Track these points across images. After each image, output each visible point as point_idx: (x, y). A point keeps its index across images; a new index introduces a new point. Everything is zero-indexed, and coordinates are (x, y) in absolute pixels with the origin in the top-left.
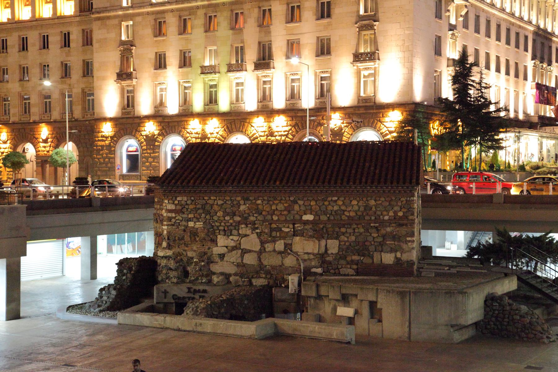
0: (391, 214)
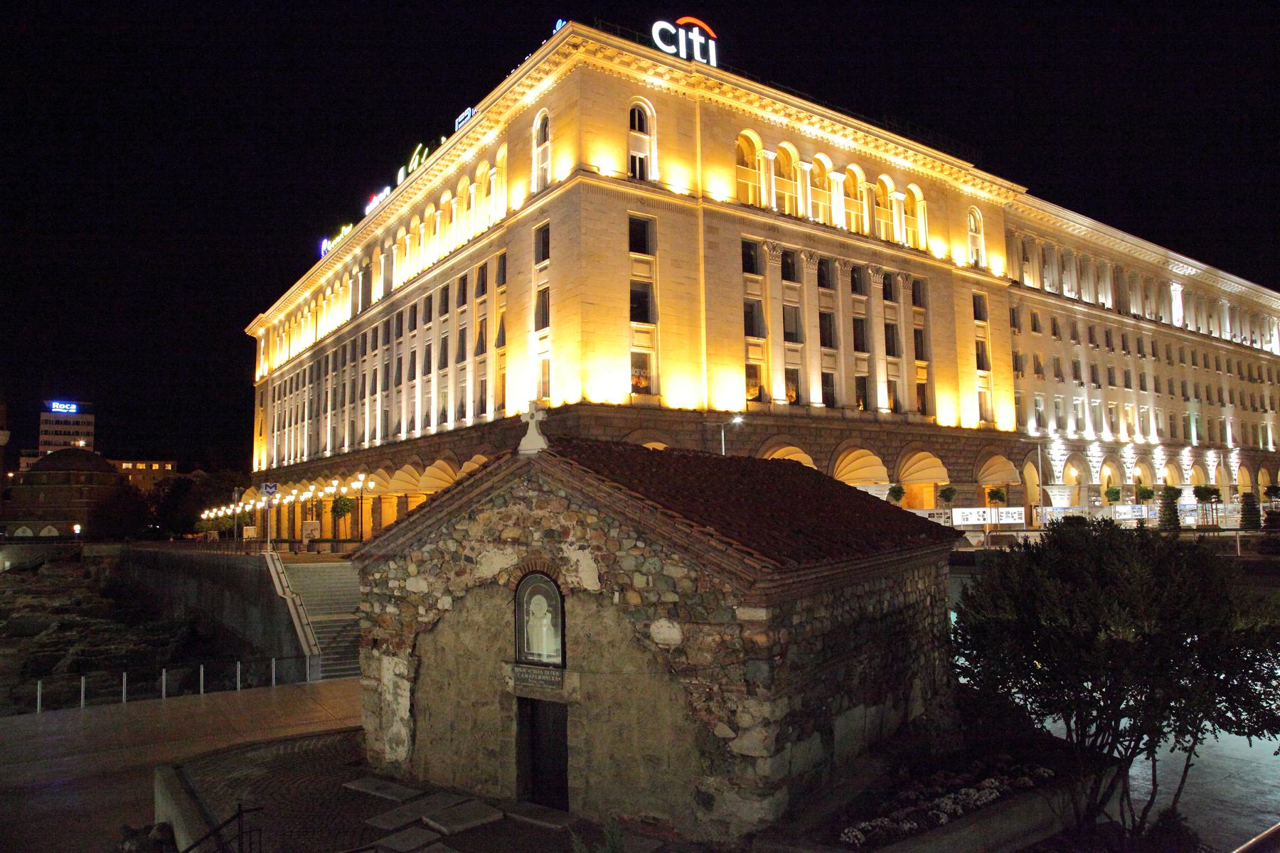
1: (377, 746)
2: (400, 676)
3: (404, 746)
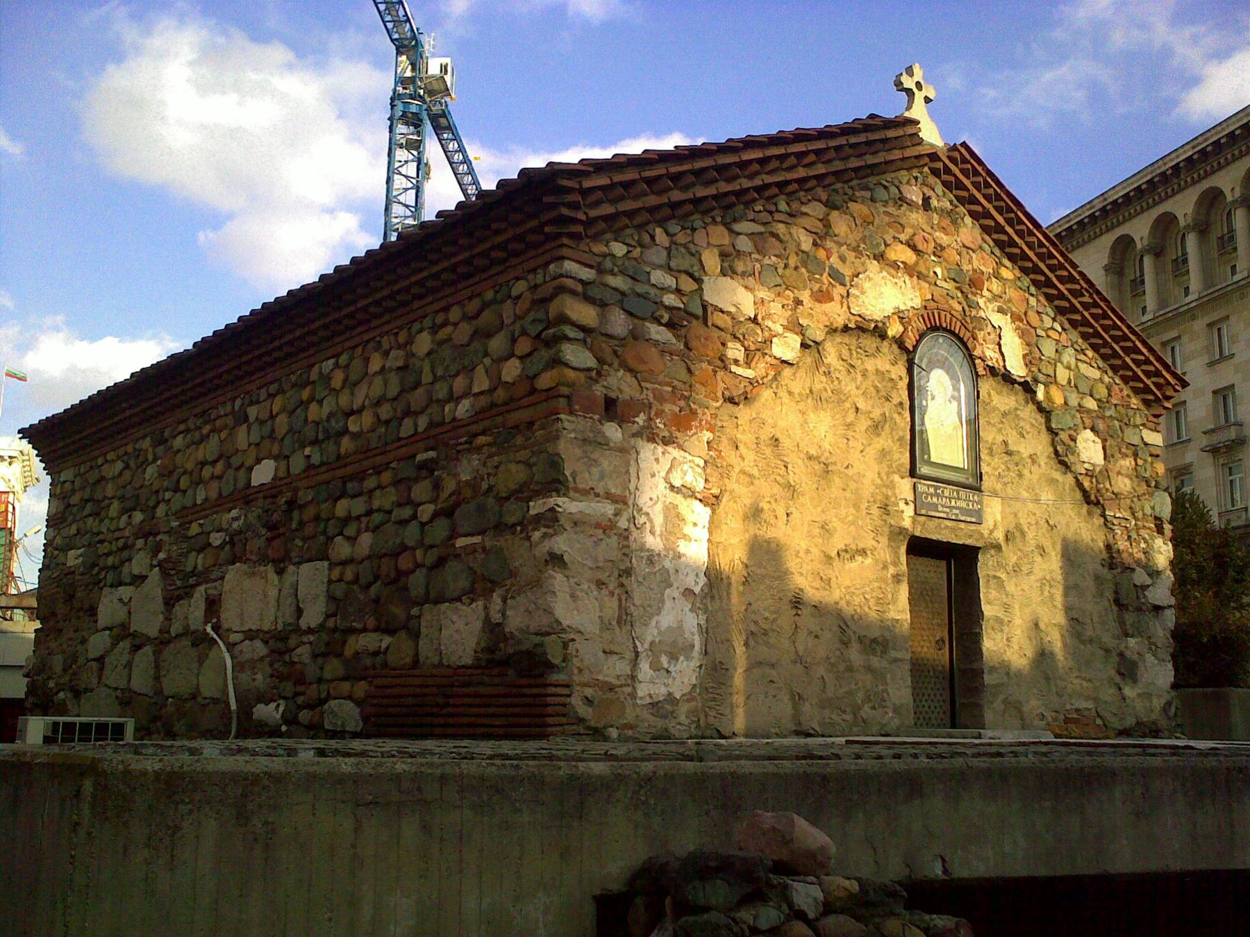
0: (481, 382)
1: (615, 669)
2: (687, 492)
3: (688, 658)
